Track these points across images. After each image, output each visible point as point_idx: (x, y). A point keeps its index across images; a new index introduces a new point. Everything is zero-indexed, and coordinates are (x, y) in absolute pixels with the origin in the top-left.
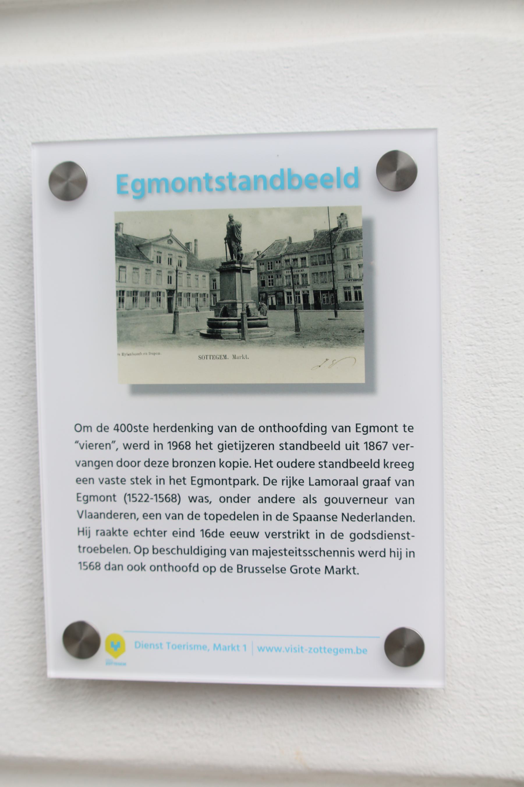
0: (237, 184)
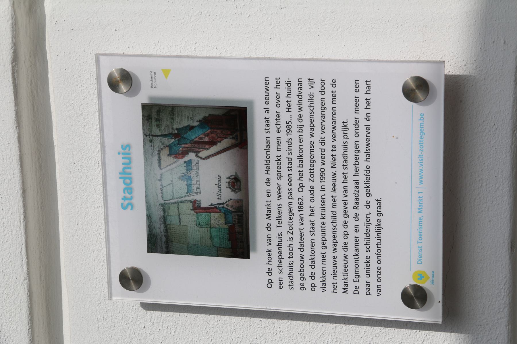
0: (129, 196)
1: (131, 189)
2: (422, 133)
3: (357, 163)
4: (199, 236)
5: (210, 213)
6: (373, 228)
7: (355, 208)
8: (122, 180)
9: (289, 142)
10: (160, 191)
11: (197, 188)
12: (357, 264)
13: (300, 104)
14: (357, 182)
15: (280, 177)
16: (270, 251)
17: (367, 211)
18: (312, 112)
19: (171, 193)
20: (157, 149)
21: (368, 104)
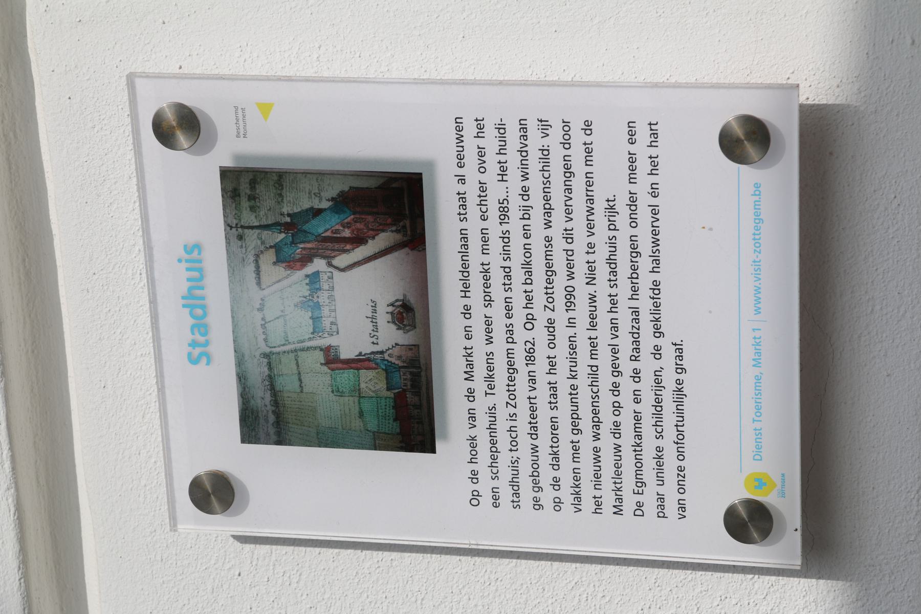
0: (201, 339)
1: (206, 326)
2: (758, 219)
3: (635, 276)
4: (339, 413)
5: (358, 369)
7: (633, 358)
8: (187, 310)
9: (505, 237)
11: (332, 323)
12: (639, 462)
13: (524, 166)
14: (636, 312)
17: (657, 365)
18: (547, 182)
21: (655, 166)
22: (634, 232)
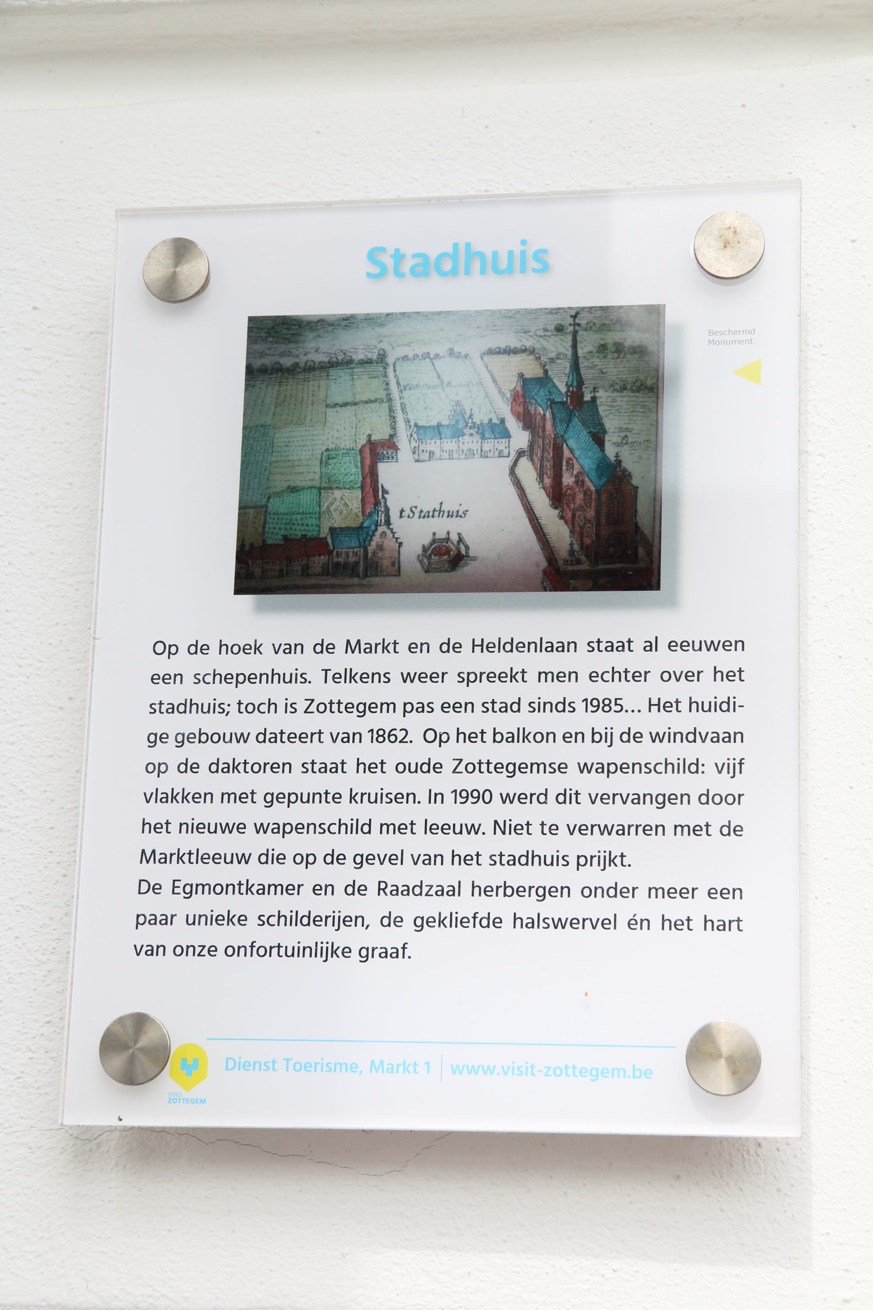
0: (406, 267)
1: (426, 275)
3: (509, 891)
4: (296, 458)
5: (363, 487)
6: (325, 934)
7: (383, 886)
8: (449, 249)
9: (565, 706)
10: (420, 352)
11: (431, 453)
12: (225, 889)
13: (673, 736)
14: (454, 891)
15: (466, 679)
16: (257, 649)
17: (373, 919)
18: (649, 769)
19: (414, 383)
20: (537, 346)
21: (676, 925)
22: (576, 892)
